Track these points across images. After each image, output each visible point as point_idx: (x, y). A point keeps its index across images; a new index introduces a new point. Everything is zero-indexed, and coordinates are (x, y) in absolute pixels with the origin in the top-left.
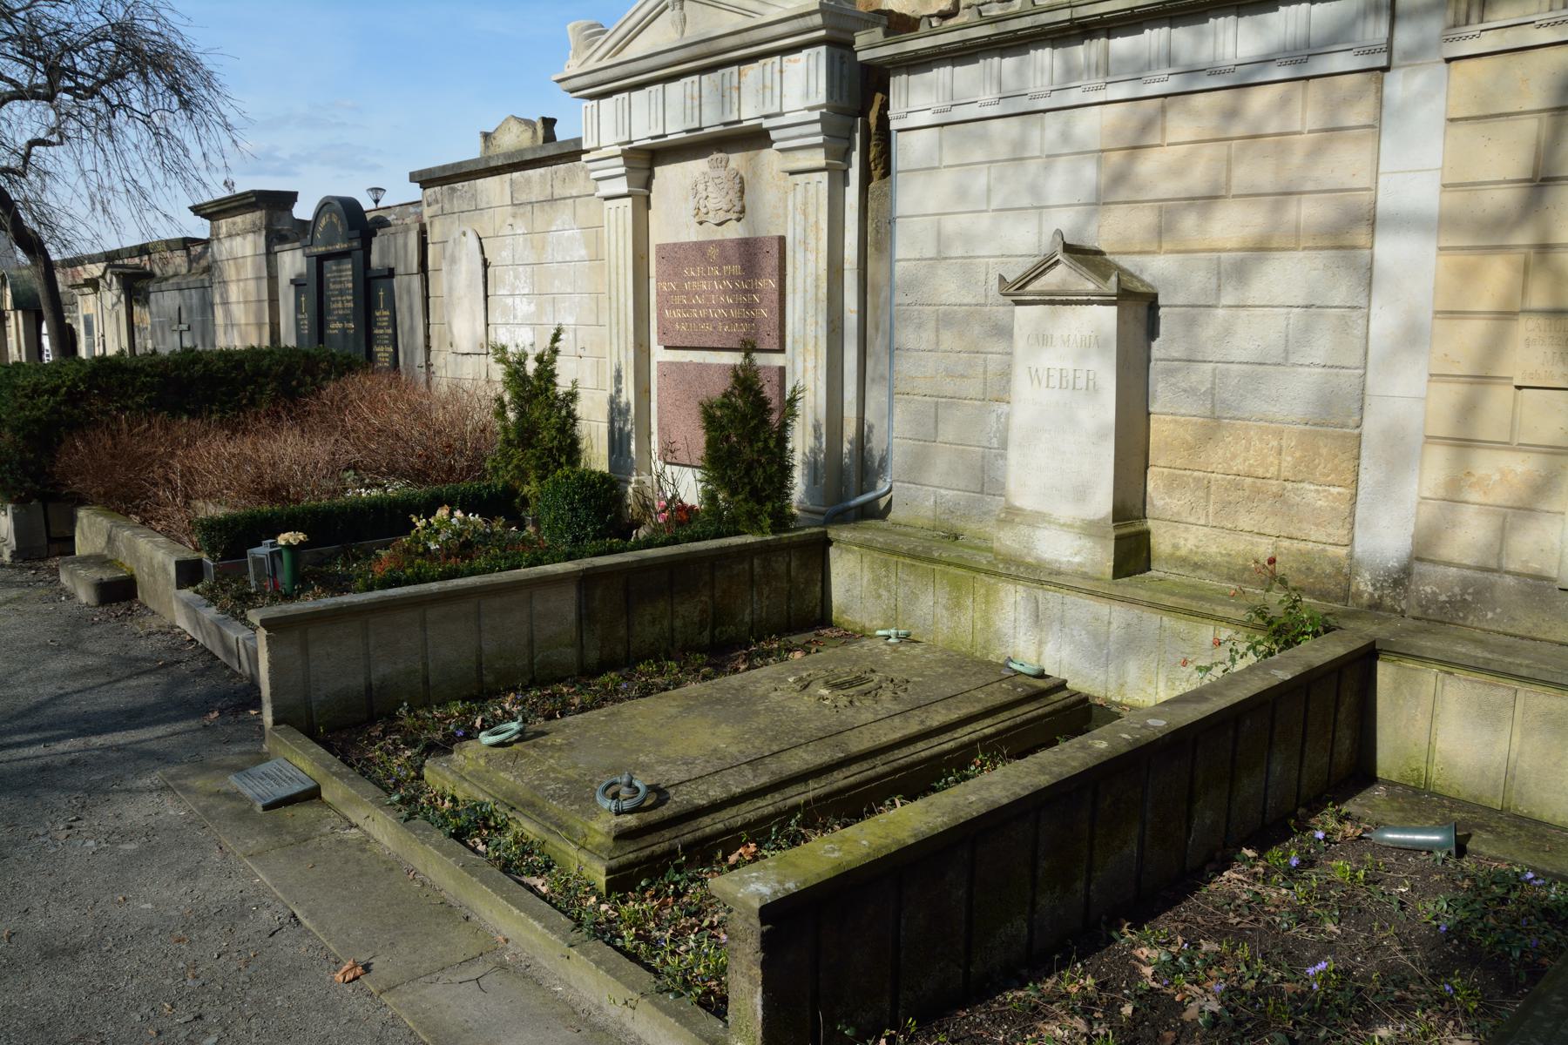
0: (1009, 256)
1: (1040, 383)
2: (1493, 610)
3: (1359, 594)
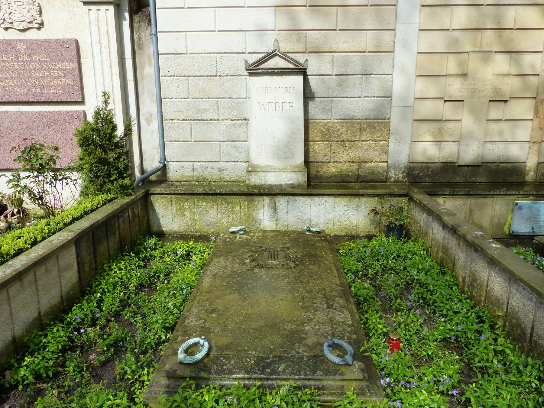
0: (228, 53)
1: (264, 109)
2: (437, 176)
3: (390, 178)
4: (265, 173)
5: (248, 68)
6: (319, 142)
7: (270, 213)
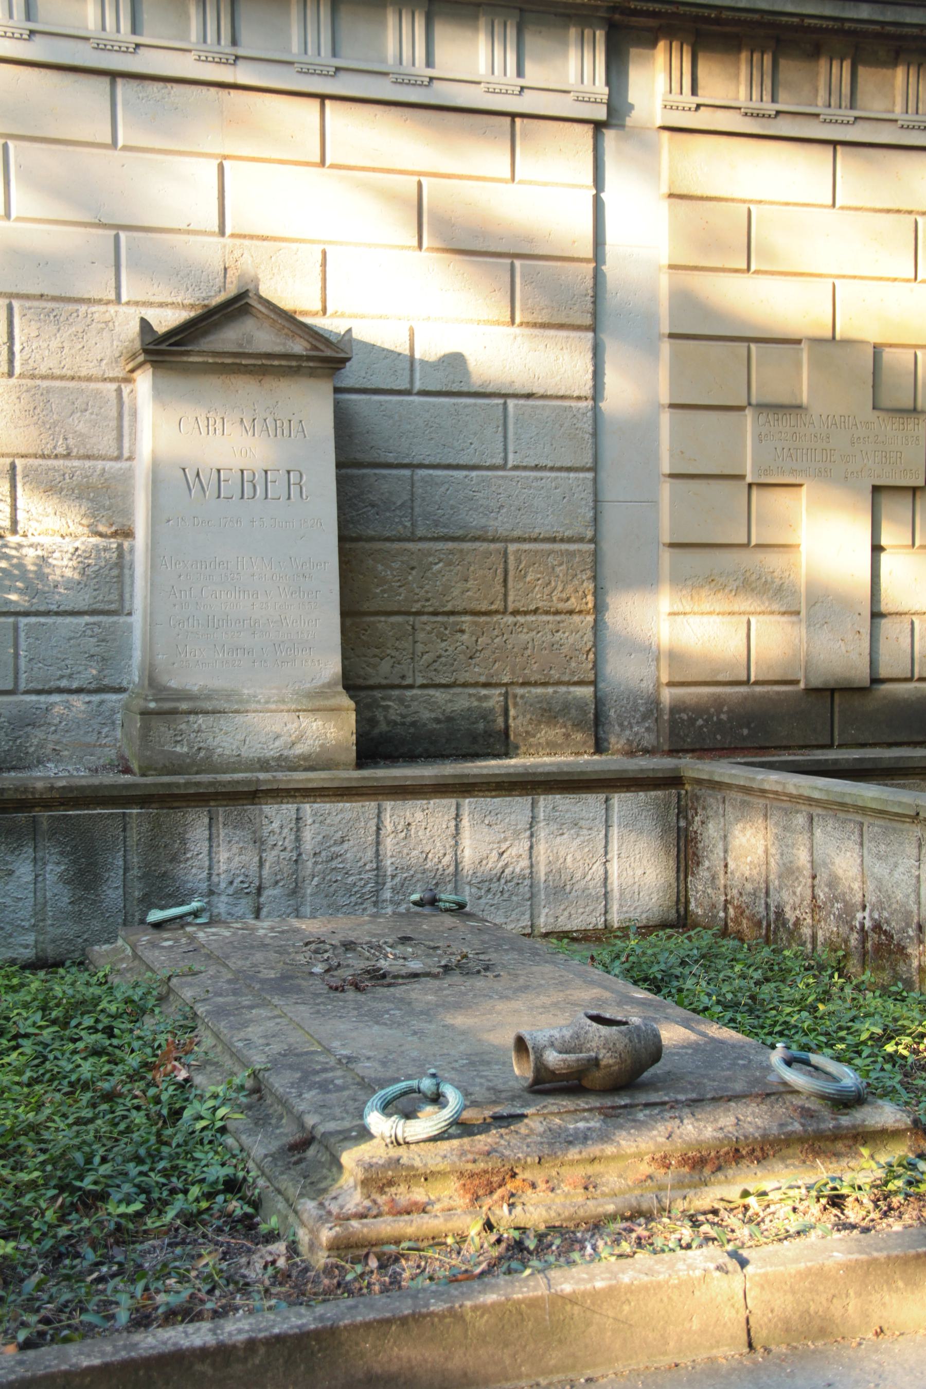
2: (748, 727)
4: (211, 718)
5: (151, 347)
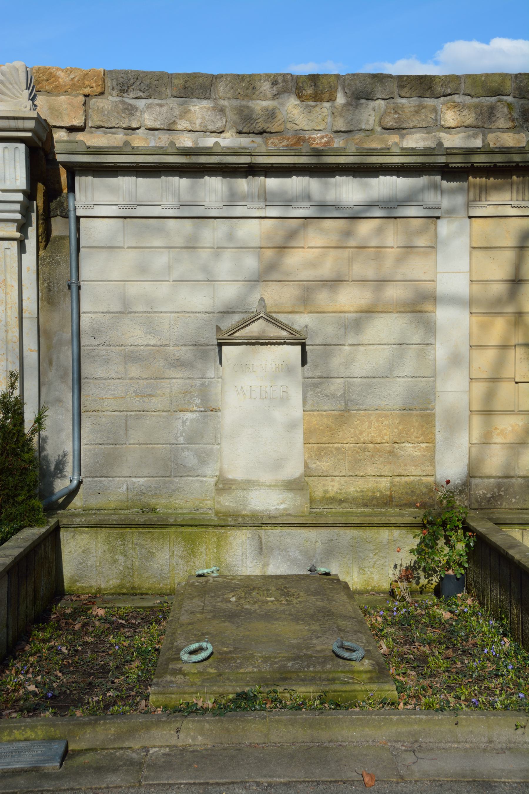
1: (244, 394)
2: (515, 498)
6: (326, 445)
7: (252, 555)
